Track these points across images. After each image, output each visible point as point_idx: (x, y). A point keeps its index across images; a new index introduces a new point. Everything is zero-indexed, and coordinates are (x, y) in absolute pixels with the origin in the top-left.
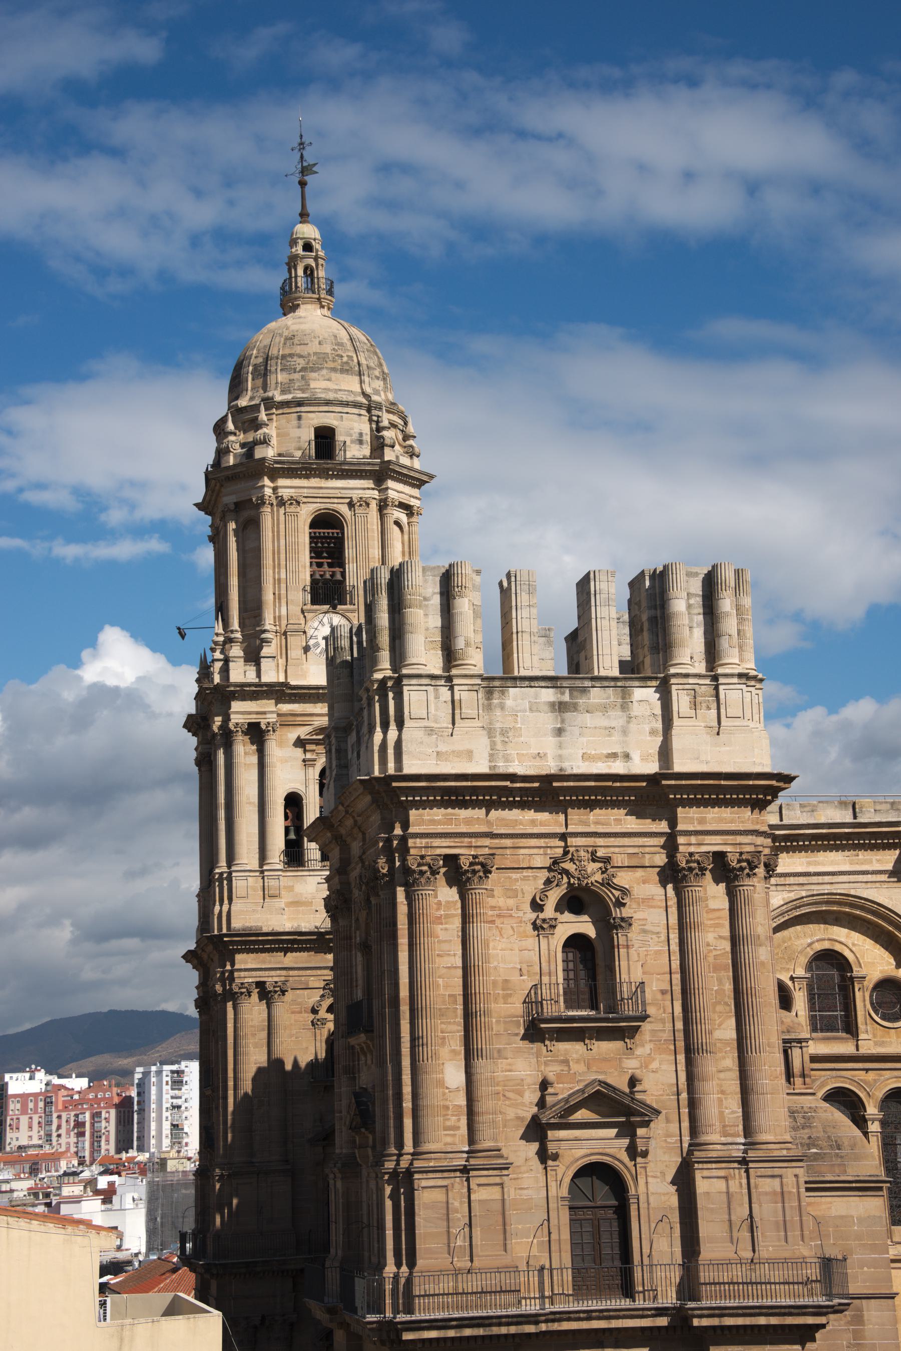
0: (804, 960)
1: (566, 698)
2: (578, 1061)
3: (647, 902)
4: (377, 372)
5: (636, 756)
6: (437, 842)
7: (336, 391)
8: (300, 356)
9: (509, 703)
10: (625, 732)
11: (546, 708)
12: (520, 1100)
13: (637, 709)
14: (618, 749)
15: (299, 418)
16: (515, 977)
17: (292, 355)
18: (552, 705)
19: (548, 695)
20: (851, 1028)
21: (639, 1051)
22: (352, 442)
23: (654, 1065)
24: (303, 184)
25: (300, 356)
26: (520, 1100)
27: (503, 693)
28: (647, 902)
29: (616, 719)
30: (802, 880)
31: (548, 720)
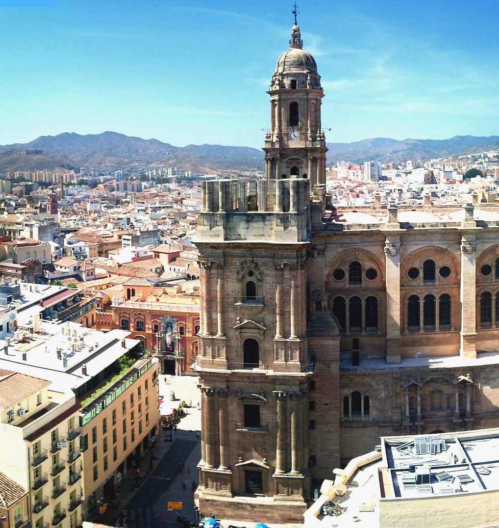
0: (348, 264)
3: (267, 275)
16: (231, 293)
20: (360, 281)
21: (263, 313)
23: (267, 316)
28: (267, 275)
30: (347, 245)
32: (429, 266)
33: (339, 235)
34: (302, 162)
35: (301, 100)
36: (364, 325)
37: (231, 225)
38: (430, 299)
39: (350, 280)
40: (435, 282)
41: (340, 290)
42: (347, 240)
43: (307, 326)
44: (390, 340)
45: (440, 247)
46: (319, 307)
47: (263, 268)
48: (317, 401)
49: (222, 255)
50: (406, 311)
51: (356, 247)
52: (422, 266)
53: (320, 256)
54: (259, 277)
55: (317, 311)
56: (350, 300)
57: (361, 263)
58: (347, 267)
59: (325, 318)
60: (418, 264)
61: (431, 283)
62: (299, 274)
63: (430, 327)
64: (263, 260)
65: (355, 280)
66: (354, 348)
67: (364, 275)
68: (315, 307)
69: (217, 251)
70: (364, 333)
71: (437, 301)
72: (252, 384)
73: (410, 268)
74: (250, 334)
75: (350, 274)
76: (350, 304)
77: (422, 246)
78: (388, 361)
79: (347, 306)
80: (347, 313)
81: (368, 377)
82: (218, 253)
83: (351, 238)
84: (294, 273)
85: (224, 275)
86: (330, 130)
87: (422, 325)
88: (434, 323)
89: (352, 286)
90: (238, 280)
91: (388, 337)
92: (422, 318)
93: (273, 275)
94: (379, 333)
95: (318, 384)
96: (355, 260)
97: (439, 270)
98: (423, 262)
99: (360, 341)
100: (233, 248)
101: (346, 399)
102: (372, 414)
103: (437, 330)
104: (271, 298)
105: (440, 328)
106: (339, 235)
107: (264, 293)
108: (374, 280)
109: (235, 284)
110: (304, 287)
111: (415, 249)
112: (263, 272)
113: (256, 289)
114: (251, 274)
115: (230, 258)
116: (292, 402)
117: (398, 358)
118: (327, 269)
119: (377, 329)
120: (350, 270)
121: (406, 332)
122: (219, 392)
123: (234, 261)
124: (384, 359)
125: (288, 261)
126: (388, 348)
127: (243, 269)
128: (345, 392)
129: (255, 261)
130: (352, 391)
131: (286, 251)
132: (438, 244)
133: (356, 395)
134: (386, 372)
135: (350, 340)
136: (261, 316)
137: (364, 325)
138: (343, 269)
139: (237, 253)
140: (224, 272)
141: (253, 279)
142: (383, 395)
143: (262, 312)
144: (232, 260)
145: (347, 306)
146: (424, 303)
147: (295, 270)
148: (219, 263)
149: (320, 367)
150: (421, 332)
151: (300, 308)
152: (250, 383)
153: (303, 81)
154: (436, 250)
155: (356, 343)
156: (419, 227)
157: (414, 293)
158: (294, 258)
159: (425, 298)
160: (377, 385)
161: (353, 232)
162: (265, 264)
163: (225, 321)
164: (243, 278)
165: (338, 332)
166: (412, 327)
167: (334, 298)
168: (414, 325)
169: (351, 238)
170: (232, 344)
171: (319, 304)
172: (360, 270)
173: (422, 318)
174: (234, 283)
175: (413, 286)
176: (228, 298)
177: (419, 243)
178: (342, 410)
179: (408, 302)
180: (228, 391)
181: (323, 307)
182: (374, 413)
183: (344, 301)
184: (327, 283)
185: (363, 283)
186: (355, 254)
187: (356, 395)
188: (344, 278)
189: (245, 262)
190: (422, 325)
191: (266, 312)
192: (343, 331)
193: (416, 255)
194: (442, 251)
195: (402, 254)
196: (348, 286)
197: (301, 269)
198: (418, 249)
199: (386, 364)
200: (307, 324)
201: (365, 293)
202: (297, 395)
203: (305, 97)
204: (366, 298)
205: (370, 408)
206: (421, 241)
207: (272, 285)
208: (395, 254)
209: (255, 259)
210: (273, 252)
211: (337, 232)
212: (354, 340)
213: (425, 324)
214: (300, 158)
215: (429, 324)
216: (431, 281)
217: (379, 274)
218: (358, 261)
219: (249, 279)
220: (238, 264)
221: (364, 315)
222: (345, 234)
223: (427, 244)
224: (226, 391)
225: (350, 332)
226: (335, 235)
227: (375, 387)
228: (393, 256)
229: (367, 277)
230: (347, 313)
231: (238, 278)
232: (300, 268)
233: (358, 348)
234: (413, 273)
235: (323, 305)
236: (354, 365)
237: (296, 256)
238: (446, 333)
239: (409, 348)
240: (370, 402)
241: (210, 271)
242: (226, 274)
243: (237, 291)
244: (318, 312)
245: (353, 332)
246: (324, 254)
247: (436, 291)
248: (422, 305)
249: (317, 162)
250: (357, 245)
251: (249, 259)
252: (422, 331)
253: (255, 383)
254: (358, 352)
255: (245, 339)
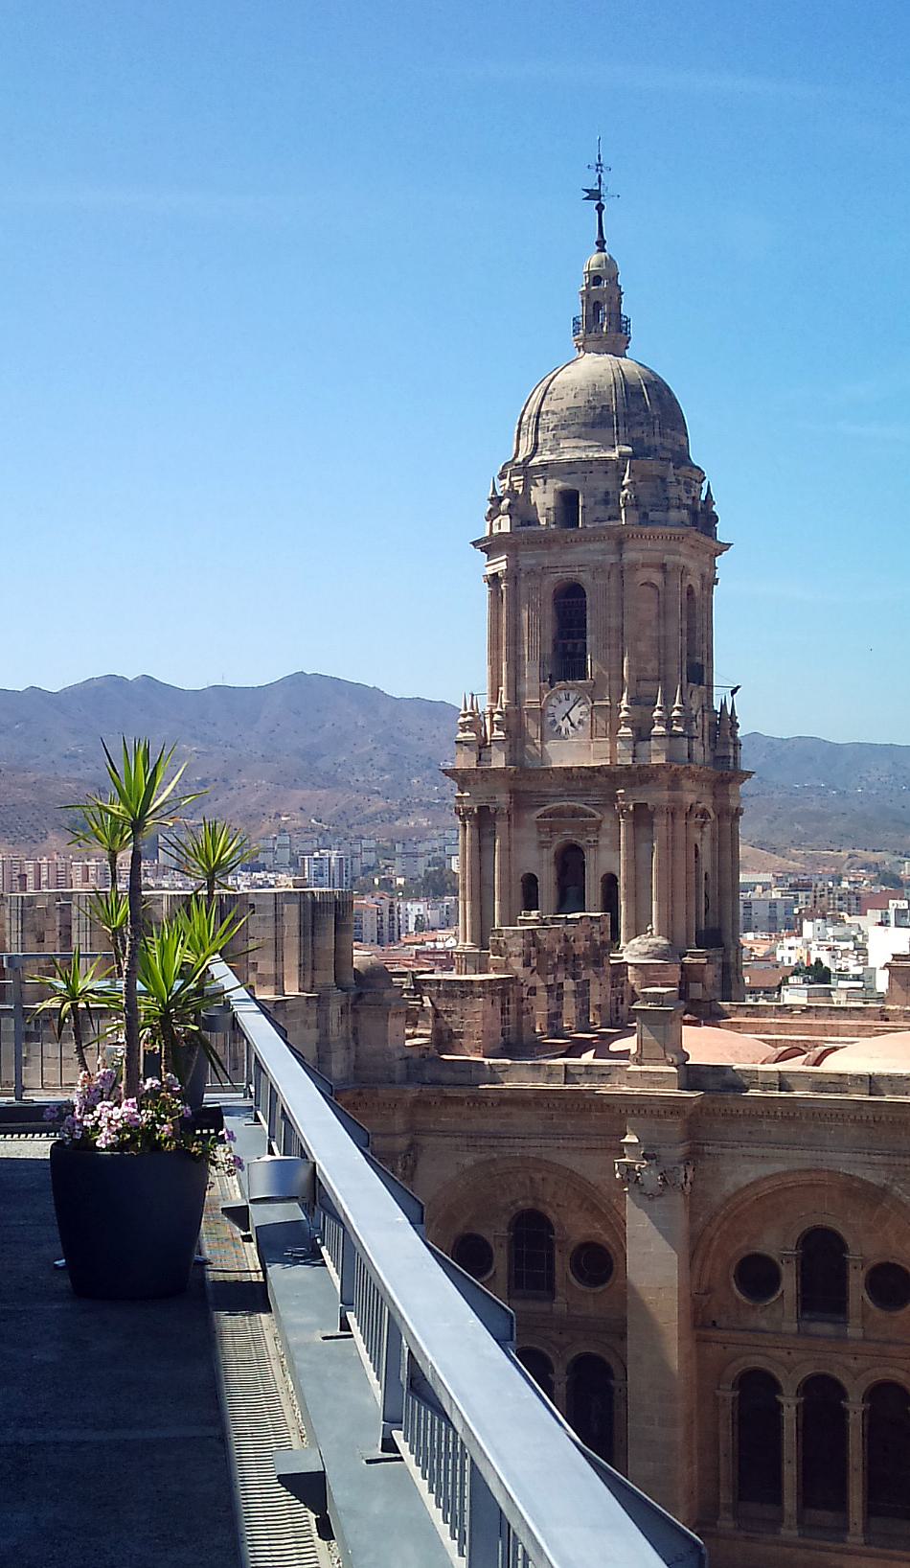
30: (494, 1142)
33: (459, 1101)
40: (846, 1323)
42: (491, 1124)
45: (861, 1180)
50: (727, 1435)
58: (503, 1231)
60: (777, 1242)
61: (827, 1328)
63: (825, 1517)
67: (562, 1265)
71: (855, 1409)
73: (746, 1253)
77: (780, 1167)
83: (508, 1115)
87: (790, 1503)
92: (790, 1472)
96: (530, 1203)
97: (862, 1274)
98: (797, 1234)
103: (855, 1538)
105: (866, 1530)
106: (459, 1101)
111: (752, 1176)
132: (845, 1162)
138: (486, 1234)
150: (783, 1531)
156: (766, 1087)
157: (758, 1362)
161: (507, 1094)
169: (508, 1115)
172: (551, 1245)
173: (790, 1472)
175: (755, 1330)
177: (767, 1151)
185: (558, 1298)
186: (532, 1180)
188: (491, 1273)
190: (790, 1503)
198: (766, 1178)
206: (777, 1144)
208: (660, 1190)
211: (450, 1092)
218: (542, 1207)
222: (479, 1101)
223: (797, 1159)
226: (448, 1100)
228: (651, 1197)
238: (893, 1558)
247: (851, 1363)
248: (789, 1414)
250: (527, 1142)
252: (789, 1532)
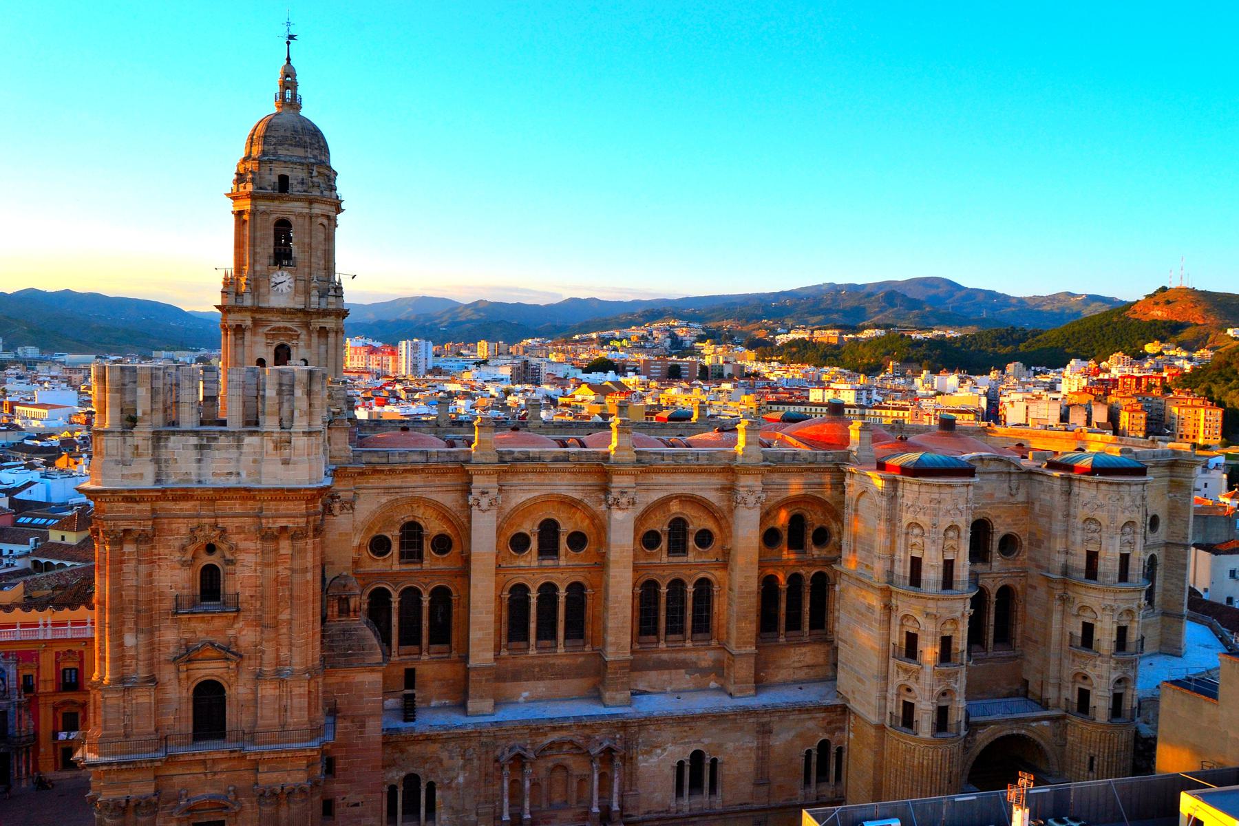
0: (399, 526)
1: (205, 442)
2: (201, 631)
3: (246, 551)
4: (316, 146)
5: (244, 474)
6: (120, 523)
7: (291, 156)
8: (274, 137)
9: (170, 445)
10: (238, 461)
11: (192, 447)
12: (167, 651)
13: (245, 449)
14: (234, 470)
15: (271, 170)
16: (168, 590)
17: (270, 136)
18: (196, 446)
19: (194, 440)
20: (420, 557)
21: (236, 626)
22: (298, 183)
23: (244, 633)
24: (288, 43)
25: (274, 137)
26: (167, 651)
27: (167, 439)
29: (233, 453)
30: (397, 490)
31: (193, 454)
32: (549, 530)
34: (299, 335)
35: (300, 215)
36: (425, 641)
37: (164, 454)
38: (548, 591)
39: (401, 555)
40: (558, 559)
41: (381, 575)
43: (322, 648)
44: (475, 668)
46: (345, 610)
47: (235, 539)
48: (339, 800)
49: (149, 514)
50: (505, 614)
51: (414, 495)
52: (536, 529)
53: (345, 511)
54: (228, 556)
55: (339, 616)
56: (402, 594)
57: (422, 523)
58: (397, 532)
59: (355, 629)
60: (529, 527)
62: (310, 546)
63: (547, 643)
64: (238, 522)
65: (410, 555)
66: (406, 688)
67: (427, 546)
68: (336, 609)
69: (137, 507)
70: (425, 657)
72: (209, 777)
74: (208, 672)
75: (402, 545)
76: (400, 602)
77: (537, 494)
78: (470, 710)
79: (393, 605)
80: (395, 620)
81: (435, 743)
82: (139, 511)
84: (300, 544)
85: (152, 554)
86: (353, 278)
87: (532, 640)
88: (554, 636)
89: (405, 567)
90: (184, 564)
91: (472, 663)
92: (533, 626)
93: (257, 549)
94: (454, 655)
95: (340, 764)
96: (411, 519)
97: (566, 537)
98: (539, 522)
99: (417, 673)
100: (173, 500)
101: (392, 790)
102: (440, 820)
104: (252, 596)
107: (239, 586)
108: (446, 555)
109: (177, 572)
110: (318, 571)
111: (523, 499)
112: (237, 546)
113: (222, 579)
114: (211, 549)
115: (166, 520)
116: (292, 806)
117: (488, 705)
118: (357, 537)
119: (451, 647)
120: (402, 537)
121: (504, 653)
122: (138, 805)
123: (174, 526)
124: (462, 707)
125: (289, 521)
126: (471, 684)
127: (193, 540)
128: (390, 775)
129: (220, 525)
130: (403, 774)
131: (286, 503)
133: (412, 781)
134: (468, 733)
135: (399, 672)
136: (231, 632)
137: (425, 641)
138: (388, 535)
139: (181, 510)
140: (153, 547)
141: (213, 559)
142: (461, 779)
143: (233, 623)
144: (170, 523)
145: (395, 605)
146: (538, 598)
147: (301, 538)
148: (143, 530)
149: (346, 728)
151: (311, 613)
152: (205, 774)
153: (303, 179)
154: (562, 503)
155: (410, 678)
157: (521, 581)
158: (302, 516)
159: (540, 590)
160: (451, 758)
162: (240, 529)
163: (154, 649)
164: (194, 558)
165: (381, 656)
166: (514, 644)
167: (369, 591)
168: (519, 640)
170: (168, 696)
171: (343, 601)
172: (421, 537)
173: (533, 626)
174: (173, 568)
176: (160, 600)
178: (385, 814)
179: (509, 596)
180: (159, 799)
181: (352, 609)
182: (444, 817)
183: (389, 595)
184: (356, 562)
187: (412, 781)
188: (390, 553)
189: (200, 527)
190: (532, 640)
191: (241, 624)
192: (387, 654)
193: (524, 510)
194: (571, 504)
195: (500, 509)
196: (396, 567)
197: (315, 536)
199: (467, 716)
200: (322, 643)
201: (427, 580)
202: (302, 791)
203: (306, 210)
204: (430, 589)
205: (437, 807)
207: (256, 570)
209: (220, 520)
210: (259, 504)
212: (407, 670)
213: (538, 637)
214: (295, 328)
215: (546, 638)
216: (550, 557)
217: (456, 543)
218: (417, 520)
219: (206, 559)
220: (183, 530)
221: (425, 623)
224: (155, 799)
225: (399, 655)
227: (446, 762)
229: (434, 550)
230: (395, 620)
231: (184, 559)
232: (311, 534)
233: (412, 687)
234: (519, 543)
235: (352, 606)
236: (406, 720)
237: (304, 512)
239: (508, 684)
240: (438, 793)
241: (122, 549)
242: (156, 552)
243: (180, 585)
244: (343, 619)
245: (405, 655)
246: (353, 508)
248: (533, 601)
249: (327, 337)
250: (416, 490)
251: (207, 520)
253: (215, 773)
254: (413, 696)
255: (196, 683)
